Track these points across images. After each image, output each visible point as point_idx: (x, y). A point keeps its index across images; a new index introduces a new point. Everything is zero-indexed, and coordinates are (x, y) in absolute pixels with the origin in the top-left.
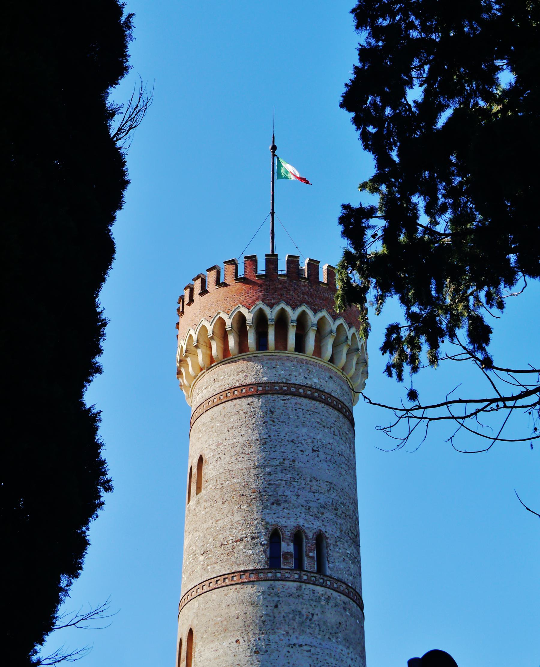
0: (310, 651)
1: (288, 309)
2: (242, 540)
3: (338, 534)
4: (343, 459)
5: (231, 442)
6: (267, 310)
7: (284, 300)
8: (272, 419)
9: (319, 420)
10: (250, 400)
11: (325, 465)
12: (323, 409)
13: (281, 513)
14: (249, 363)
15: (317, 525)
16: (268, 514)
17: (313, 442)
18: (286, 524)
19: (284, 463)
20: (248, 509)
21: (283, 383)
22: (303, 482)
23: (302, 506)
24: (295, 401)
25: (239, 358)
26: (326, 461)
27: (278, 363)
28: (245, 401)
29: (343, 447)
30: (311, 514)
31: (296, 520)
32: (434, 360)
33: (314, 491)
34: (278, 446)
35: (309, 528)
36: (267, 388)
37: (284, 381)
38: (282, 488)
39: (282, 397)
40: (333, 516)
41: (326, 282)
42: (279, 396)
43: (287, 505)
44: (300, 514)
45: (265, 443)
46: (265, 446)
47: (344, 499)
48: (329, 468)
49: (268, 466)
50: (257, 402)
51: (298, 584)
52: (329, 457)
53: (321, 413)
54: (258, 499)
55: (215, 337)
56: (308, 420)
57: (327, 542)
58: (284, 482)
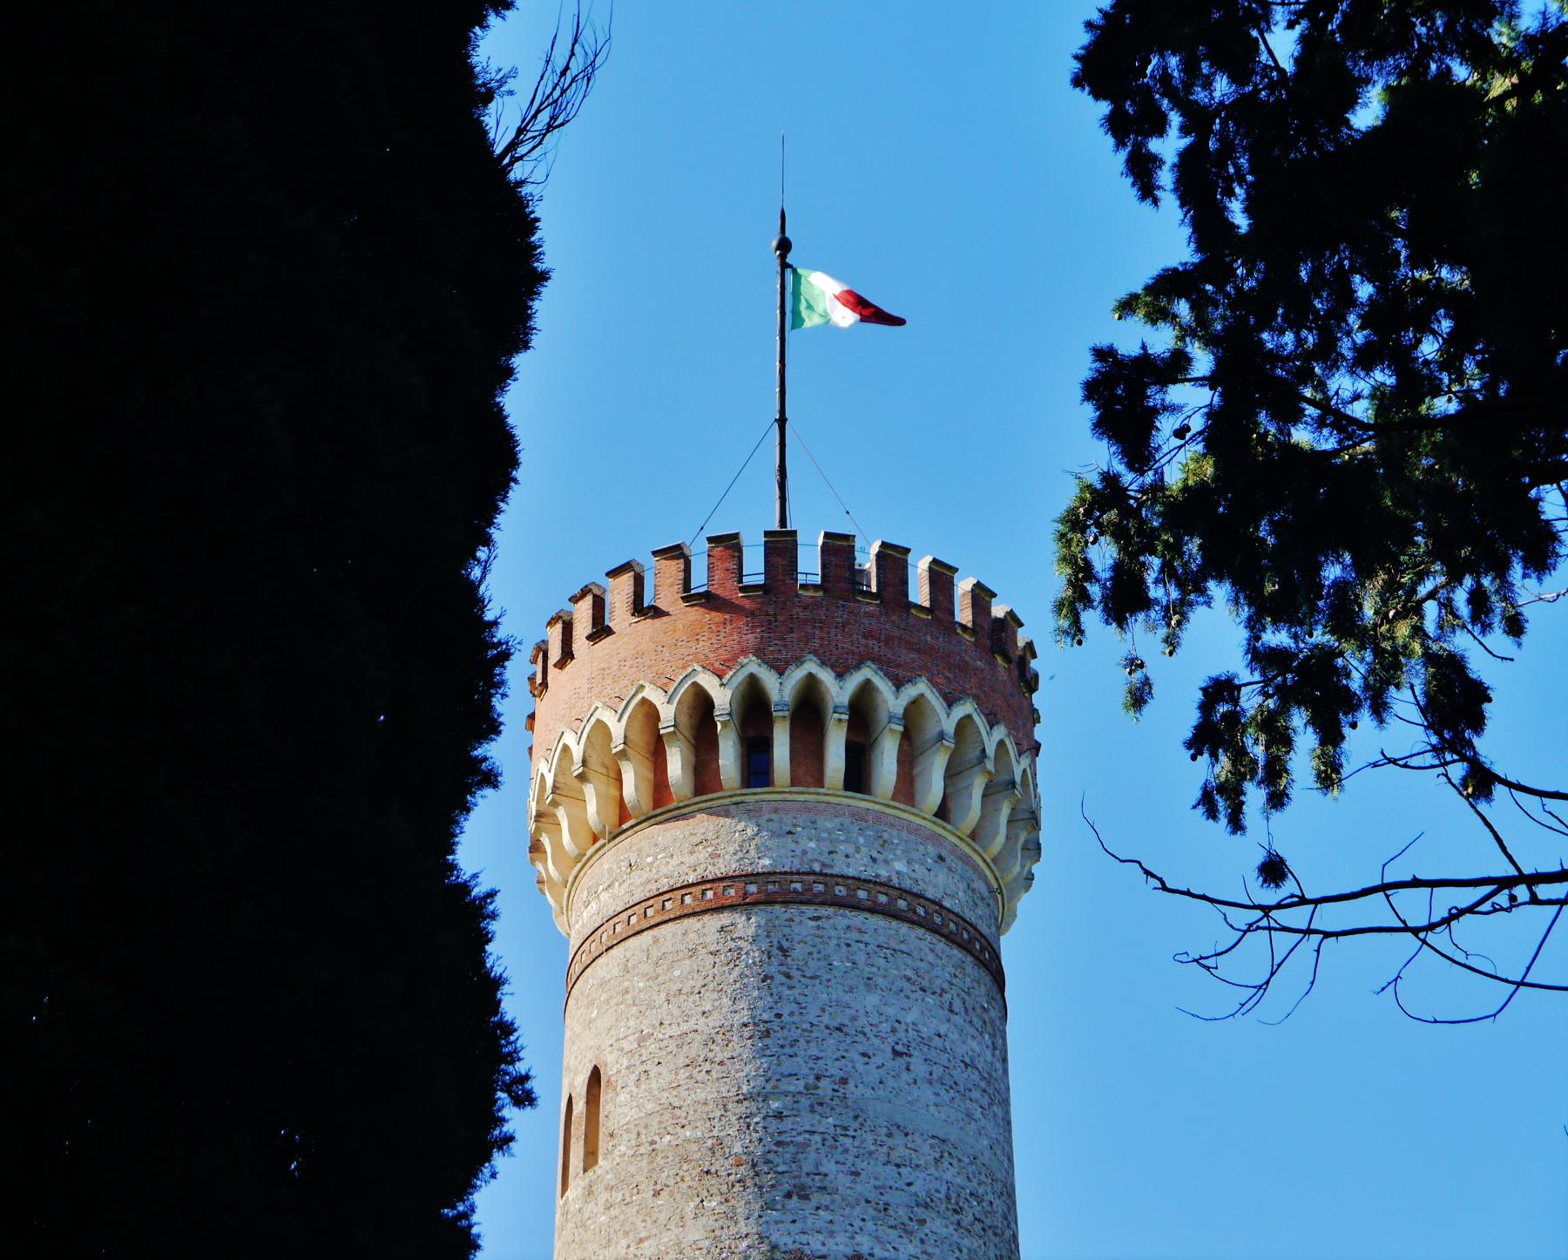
1: (826, 677)
4: (976, 1077)
5: (675, 1031)
6: (769, 679)
7: (815, 653)
8: (784, 969)
9: (909, 973)
10: (725, 918)
11: (926, 1093)
12: (922, 944)
13: (810, 1221)
14: (722, 820)
16: (776, 1222)
17: (894, 1031)
18: (824, 1250)
19: (817, 1088)
20: (723, 1208)
21: (813, 873)
22: (869, 1138)
23: (868, 1202)
24: (846, 922)
25: (695, 808)
26: (930, 1083)
27: (800, 822)
28: (713, 922)
29: (974, 1045)
30: (892, 1222)
32: (1329, 775)
37: (817, 868)
38: (813, 1155)
39: (810, 911)
40: (951, 1228)
41: (927, 604)
42: (804, 908)
43: (825, 1199)
45: (767, 1034)
46: (768, 1041)
48: (938, 1100)
49: (776, 1093)
50: (745, 925)
52: (938, 1071)
53: (915, 954)
54: (749, 1183)
55: (630, 751)
56: (882, 972)
58: (817, 1138)
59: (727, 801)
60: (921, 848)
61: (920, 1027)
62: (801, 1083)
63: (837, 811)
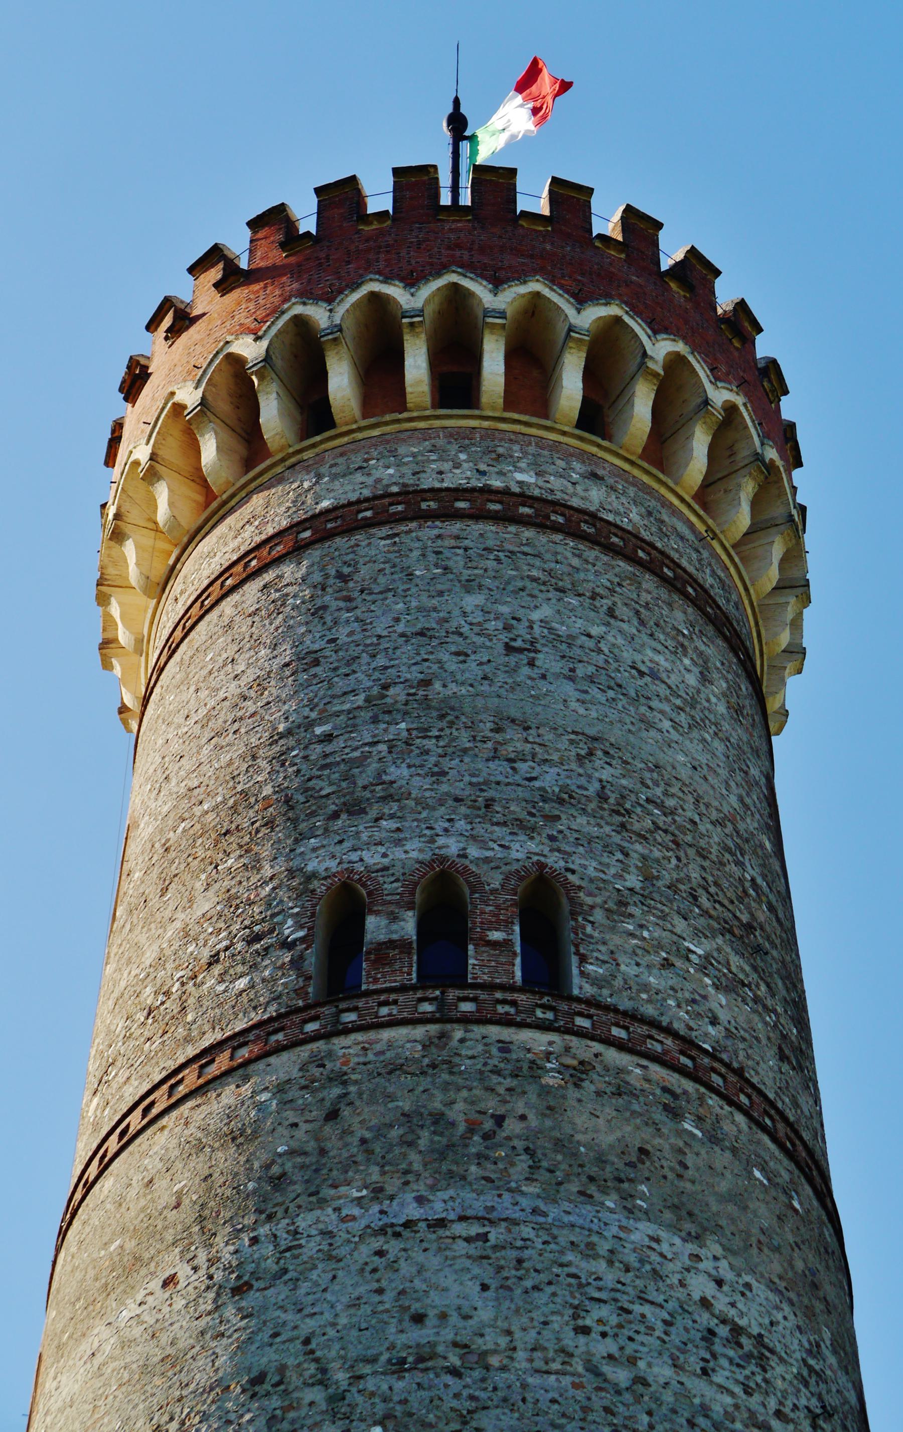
0: (484, 1237)
2: (214, 959)
3: (633, 880)
9: (535, 573)
11: (568, 688)
12: (560, 549)
15: (522, 849)
16: (314, 850)
17: (507, 628)
18: (386, 861)
19: (384, 697)
24: (436, 532)
25: (243, 494)
26: (571, 679)
28: (252, 589)
30: (498, 818)
31: (432, 841)
33: (512, 756)
34: (365, 658)
35: (487, 860)
36: (329, 526)
37: (395, 489)
39: (385, 531)
41: (546, 212)
42: (373, 531)
44: (446, 825)
45: (316, 663)
47: (666, 793)
51: (433, 1028)
53: (548, 556)
57: (571, 900)
58: (383, 747)
59: (279, 469)
60: (561, 464)
61: (554, 625)
62: (362, 697)
63: (426, 434)
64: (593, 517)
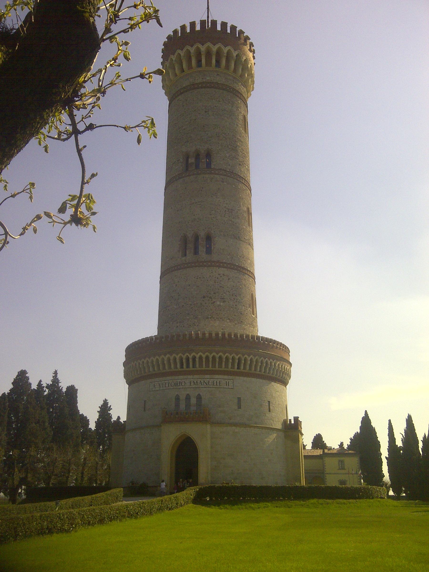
64: (217, 83)
